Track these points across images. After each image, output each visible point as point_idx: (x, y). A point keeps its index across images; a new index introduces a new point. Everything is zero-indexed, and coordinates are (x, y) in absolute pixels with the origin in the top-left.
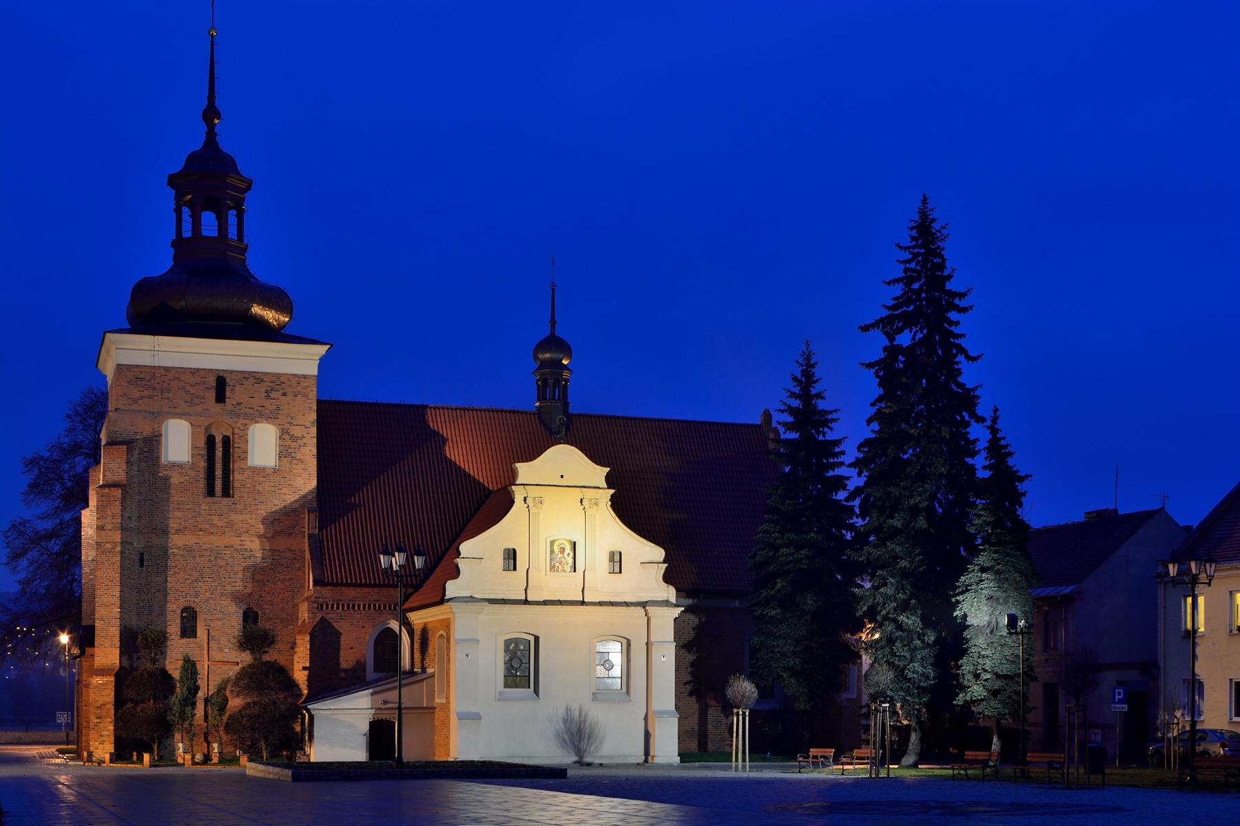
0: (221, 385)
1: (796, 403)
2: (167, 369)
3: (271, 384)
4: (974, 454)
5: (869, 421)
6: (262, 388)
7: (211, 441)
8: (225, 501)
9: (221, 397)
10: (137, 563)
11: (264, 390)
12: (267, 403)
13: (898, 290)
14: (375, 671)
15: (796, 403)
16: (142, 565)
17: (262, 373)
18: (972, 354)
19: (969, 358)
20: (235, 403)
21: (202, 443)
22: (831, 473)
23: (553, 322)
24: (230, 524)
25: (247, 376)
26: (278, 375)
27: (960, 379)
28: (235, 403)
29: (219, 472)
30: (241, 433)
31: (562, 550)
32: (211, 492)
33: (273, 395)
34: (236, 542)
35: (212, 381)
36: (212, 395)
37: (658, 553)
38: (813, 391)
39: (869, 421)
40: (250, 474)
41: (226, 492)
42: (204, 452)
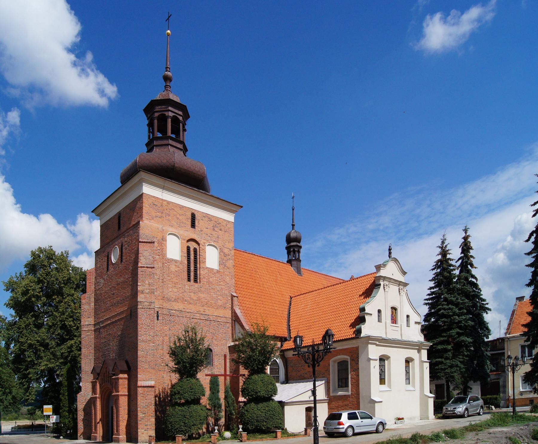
3: (216, 223)
7: (188, 248)
9: (193, 225)
10: (156, 318)
11: (212, 225)
12: (214, 233)
16: (158, 319)
17: (211, 215)
20: (200, 230)
21: (185, 251)
24: (199, 299)
25: (204, 215)
28: (200, 230)
29: (192, 268)
30: (203, 247)
32: (189, 280)
36: (189, 223)
40: (207, 271)
42: (186, 255)
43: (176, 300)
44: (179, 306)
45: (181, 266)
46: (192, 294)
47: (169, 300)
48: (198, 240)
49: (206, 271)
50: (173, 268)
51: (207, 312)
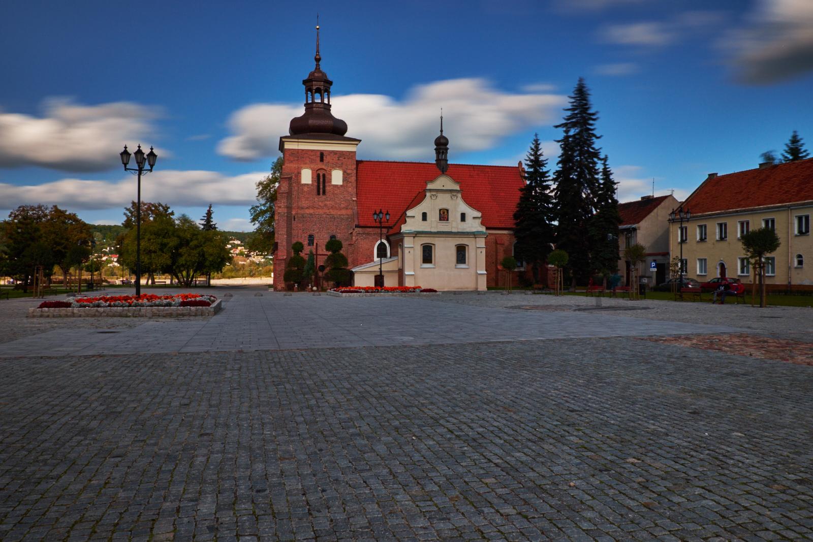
0: (322, 155)
1: (532, 158)
2: (303, 150)
4: (597, 174)
5: (558, 164)
6: (337, 156)
7: (318, 176)
8: (324, 197)
9: (322, 160)
13: (569, 113)
14: (378, 257)
15: (532, 158)
18: (598, 135)
19: (598, 138)
21: (315, 177)
22: (545, 184)
23: (442, 131)
24: (326, 205)
26: (342, 152)
27: (593, 146)
29: (321, 187)
31: (444, 213)
32: (319, 194)
33: (340, 159)
34: (327, 212)
35: (319, 154)
36: (319, 159)
37: (479, 214)
38: (538, 153)
39: (558, 164)
41: (324, 193)
42: (316, 179)
43: (307, 208)
44: (311, 211)
45: (312, 187)
46: (320, 203)
47: (302, 208)
48: (325, 168)
49: (331, 187)
50: (306, 189)
51: (332, 213)
